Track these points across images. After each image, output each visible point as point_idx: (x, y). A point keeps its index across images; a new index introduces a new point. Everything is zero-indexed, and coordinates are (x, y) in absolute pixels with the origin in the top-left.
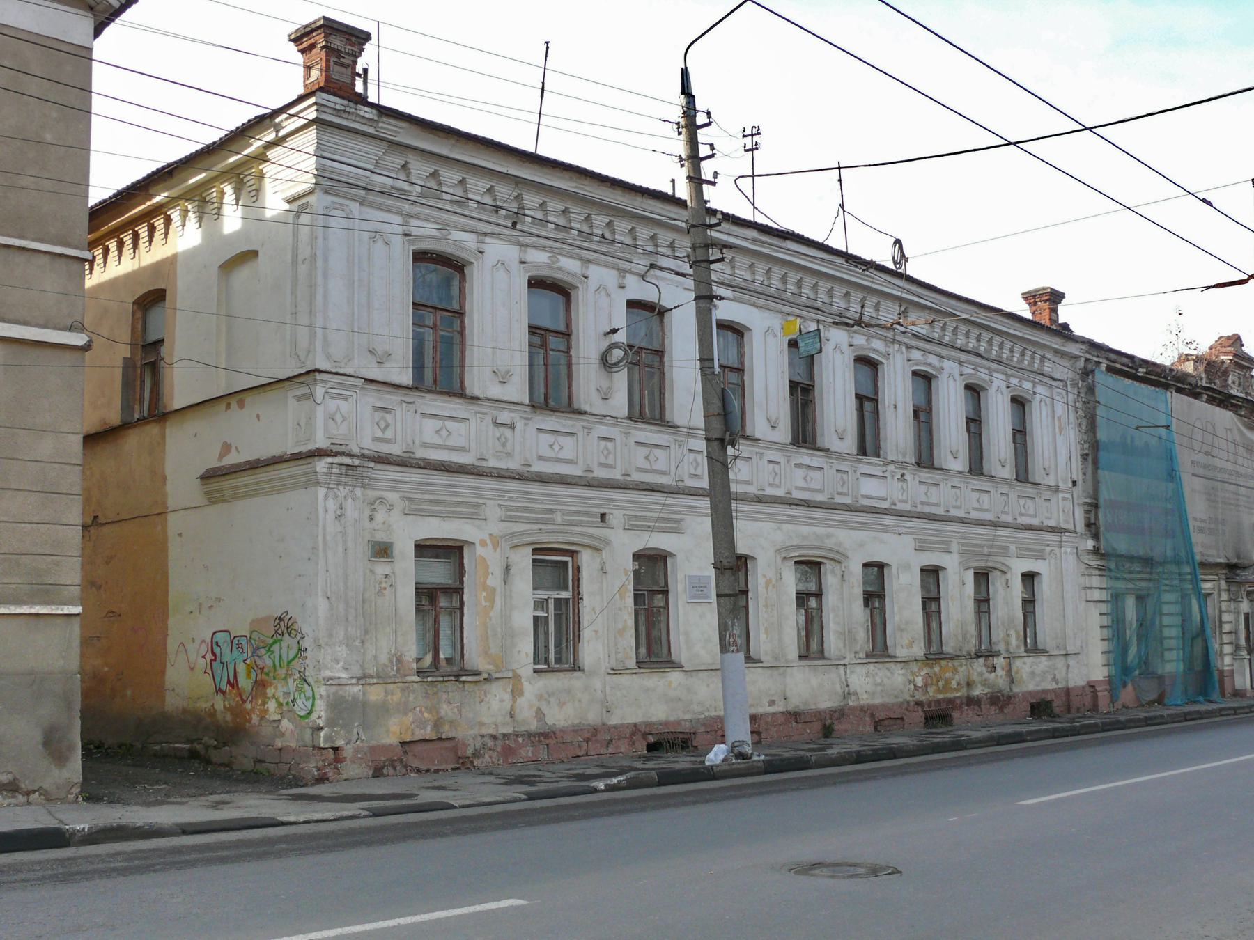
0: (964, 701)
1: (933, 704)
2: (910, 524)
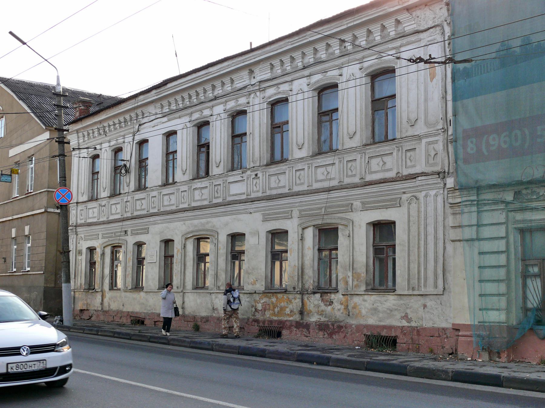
0: (294, 324)
1: (266, 323)
2: (253, 206)
